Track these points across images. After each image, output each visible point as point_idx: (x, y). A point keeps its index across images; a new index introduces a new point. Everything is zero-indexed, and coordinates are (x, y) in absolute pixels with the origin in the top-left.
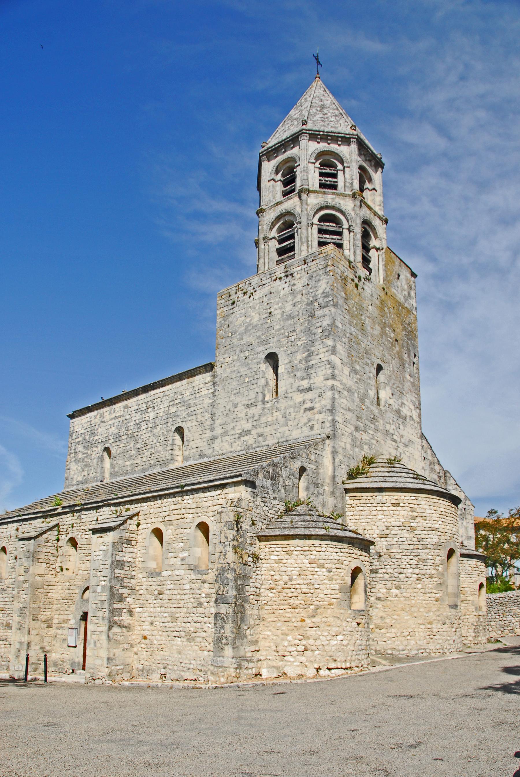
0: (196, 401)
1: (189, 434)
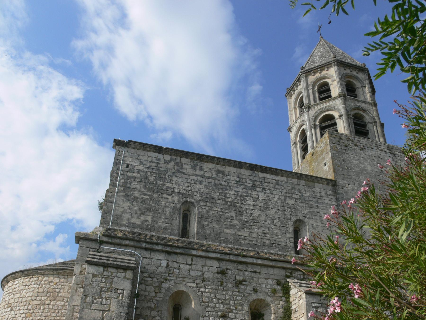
0: (318, 205)
1: (314, 231)
